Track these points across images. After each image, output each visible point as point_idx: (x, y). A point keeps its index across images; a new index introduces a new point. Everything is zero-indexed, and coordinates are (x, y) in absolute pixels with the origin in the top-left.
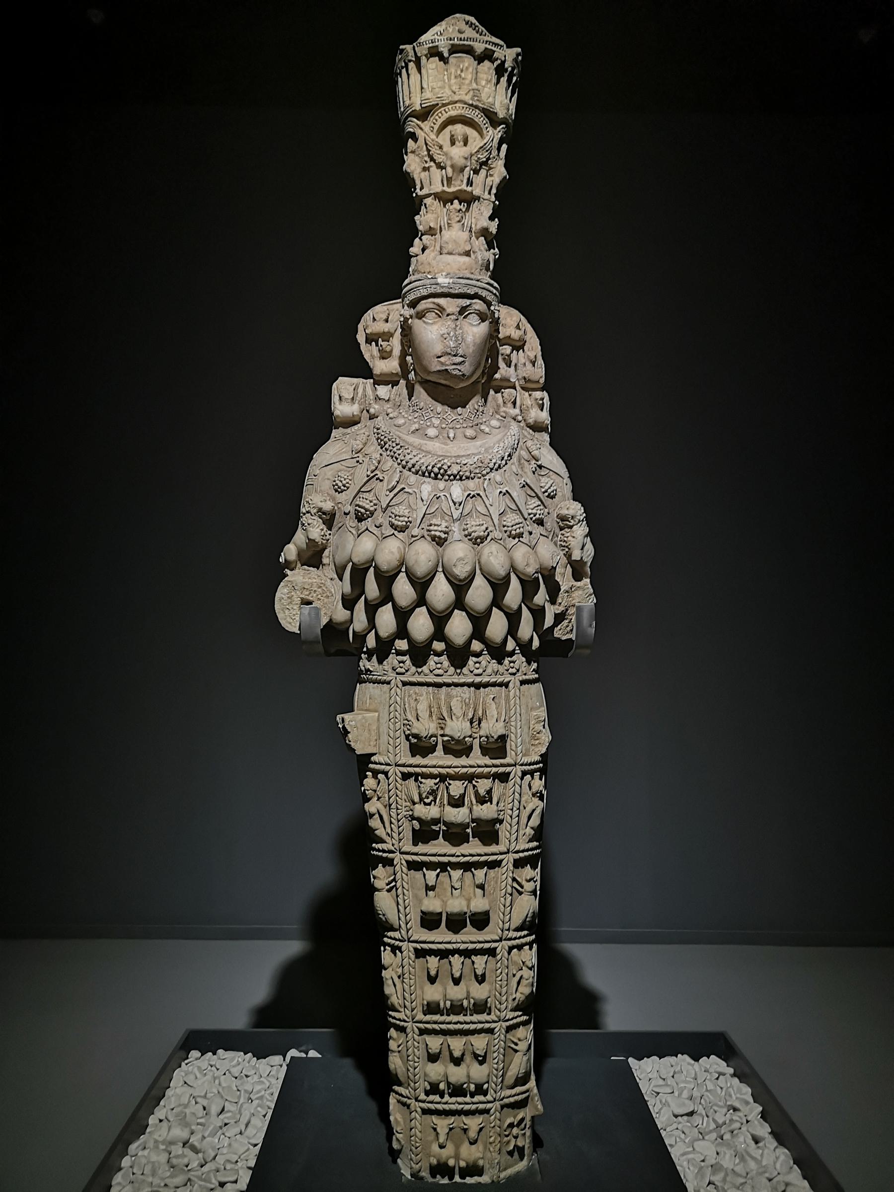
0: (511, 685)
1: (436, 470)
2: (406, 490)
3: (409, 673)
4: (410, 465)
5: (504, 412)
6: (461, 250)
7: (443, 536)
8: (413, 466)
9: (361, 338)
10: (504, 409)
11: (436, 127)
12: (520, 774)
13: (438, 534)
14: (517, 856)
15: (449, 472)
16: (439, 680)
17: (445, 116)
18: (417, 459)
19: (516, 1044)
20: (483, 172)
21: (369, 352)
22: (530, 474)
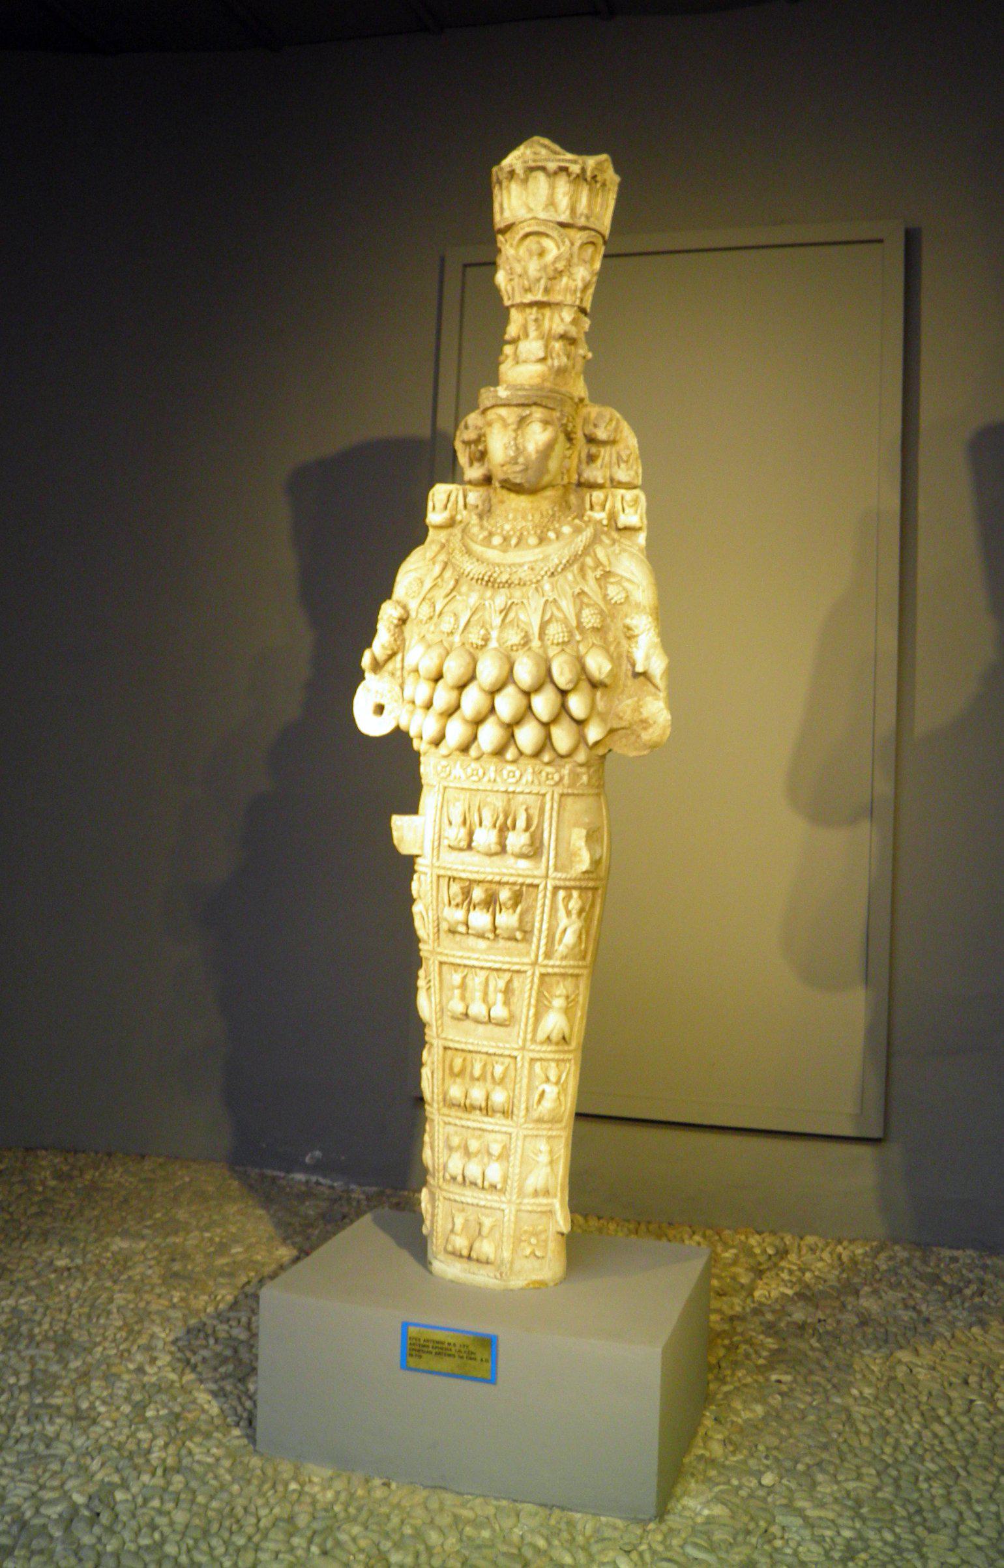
0: (548, 797)
1: (486, 578)
2: (458, 597)
5: (590, 517)
6: (533, 358)
7: (480, 643)
9: (458, 446)
10: (589, 513)
11: (515, 243)
12: (550, 888)
14: (543, 970)
16: (474, 787)
17: (522, 233)
19: (536, 1155)
20: (565, 280)
21: (463, 459)
22: (592, 582)
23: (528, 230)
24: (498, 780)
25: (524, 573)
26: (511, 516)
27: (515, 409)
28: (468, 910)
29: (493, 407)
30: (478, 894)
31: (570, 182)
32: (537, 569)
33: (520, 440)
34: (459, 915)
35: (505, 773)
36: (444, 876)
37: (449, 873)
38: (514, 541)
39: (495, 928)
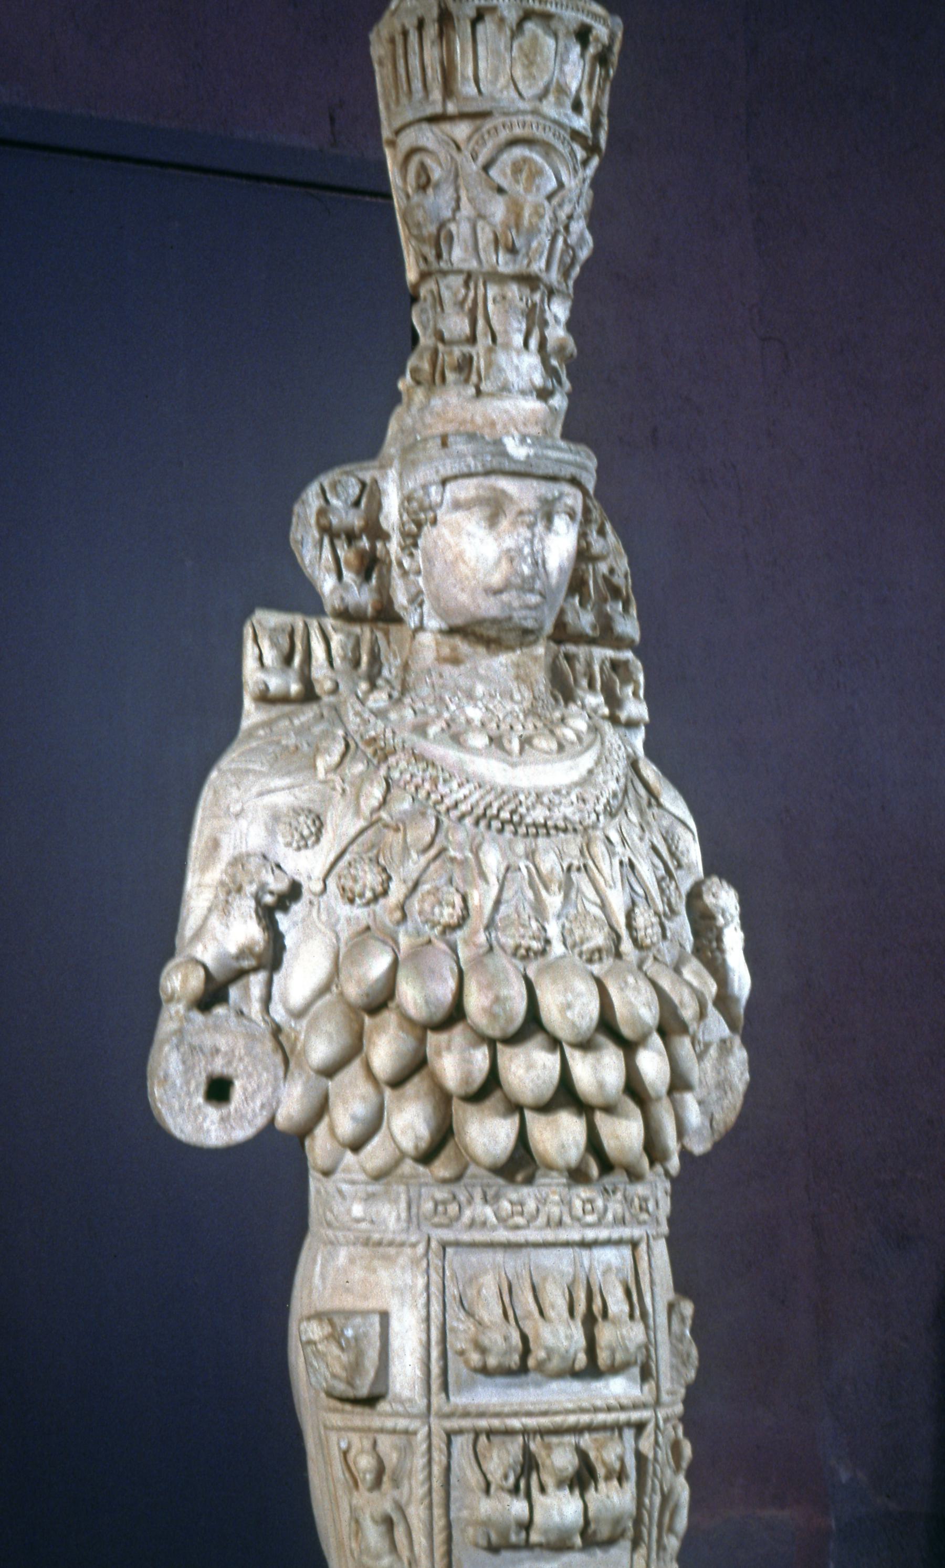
1: (505, 815)
3: (458, 1225)
4: (448, 802)
7: (535, 945)
8: (456, 805)
13: (524, 943)
15: (529, 820)
17: (504, 135)
18: (465, 791)
23: (518, 131)
24: (567, 1219)
25: (567, 810)
26: (480, 689)
27: (535, 483)
28: (528, 1496)
29: (488, 473)
30: (562, 1459)
31: (582, 55)
32: (591, 801)
33: (537, 546)
34: (519, 1507)
35: (578, 1204)
36: (460, 1432)
37: (483, 1423)
38: (515, 745)
39: (587, 1521)
